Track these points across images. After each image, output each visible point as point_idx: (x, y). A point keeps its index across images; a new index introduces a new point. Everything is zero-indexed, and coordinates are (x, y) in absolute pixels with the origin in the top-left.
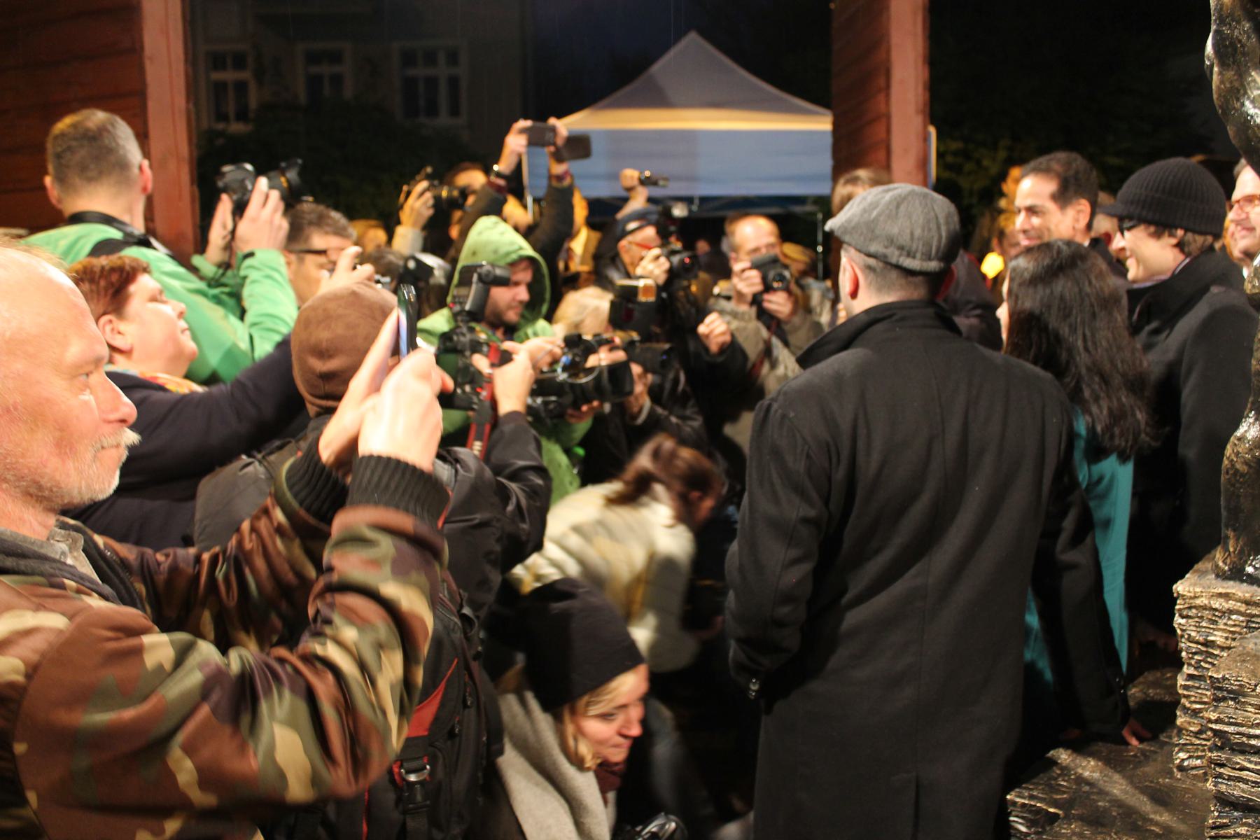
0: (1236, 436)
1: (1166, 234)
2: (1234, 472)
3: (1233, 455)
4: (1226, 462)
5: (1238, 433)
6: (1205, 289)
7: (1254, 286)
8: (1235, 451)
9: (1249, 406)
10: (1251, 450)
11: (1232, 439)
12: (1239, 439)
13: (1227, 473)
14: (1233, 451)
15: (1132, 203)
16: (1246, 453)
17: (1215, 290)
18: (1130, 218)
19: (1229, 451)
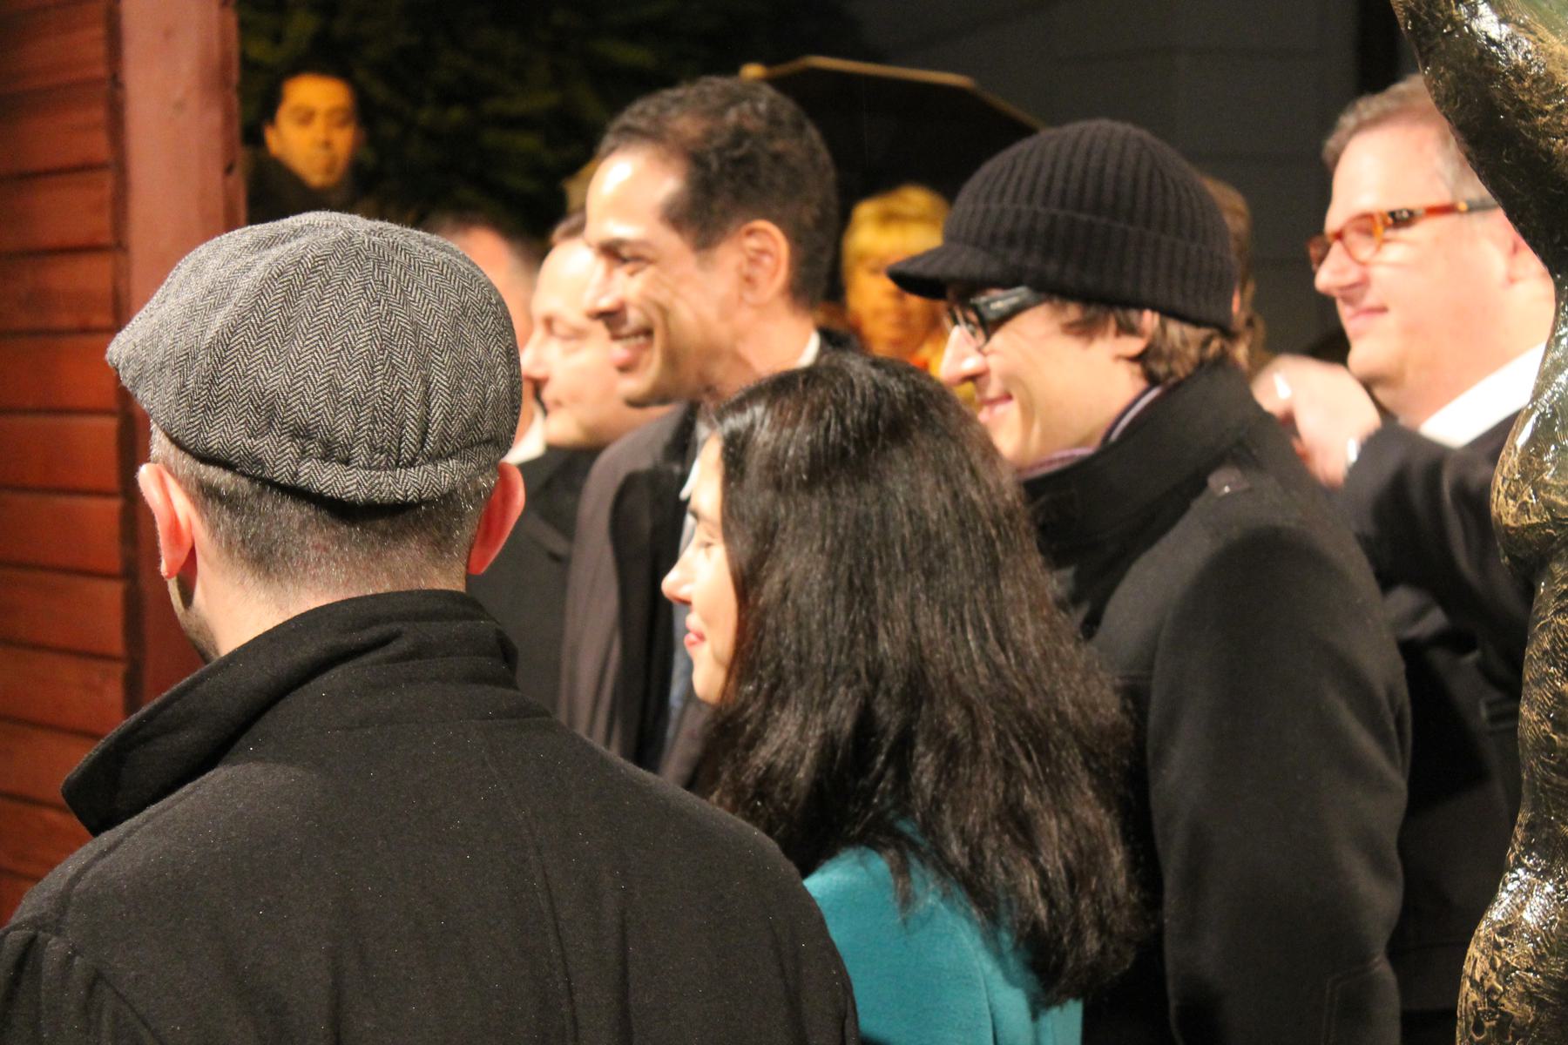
0: (1493, 924)
1: (1112, 326)
2: (1500, 1022)
3: (1493, 975)
4: (1469, 996)
5: (1496, 914)
6: (1198, 484)
7: (1524, 508)
8: (1499, 963)
9: (1519, 833)
10: (1540, 958)
11: (1483, 929)
12: (1505, 931)
13: (1478, 1028)
14: (1493, 967)
15: (1011, 240)
16: (1528, 970)
17: (1224, 483)
18: (1006, 283)
19: (1476, 960)
